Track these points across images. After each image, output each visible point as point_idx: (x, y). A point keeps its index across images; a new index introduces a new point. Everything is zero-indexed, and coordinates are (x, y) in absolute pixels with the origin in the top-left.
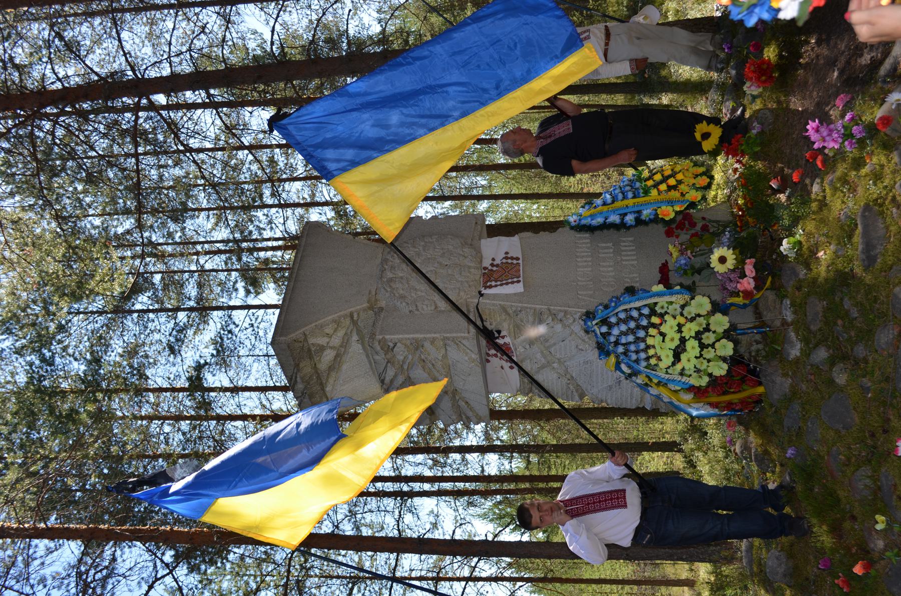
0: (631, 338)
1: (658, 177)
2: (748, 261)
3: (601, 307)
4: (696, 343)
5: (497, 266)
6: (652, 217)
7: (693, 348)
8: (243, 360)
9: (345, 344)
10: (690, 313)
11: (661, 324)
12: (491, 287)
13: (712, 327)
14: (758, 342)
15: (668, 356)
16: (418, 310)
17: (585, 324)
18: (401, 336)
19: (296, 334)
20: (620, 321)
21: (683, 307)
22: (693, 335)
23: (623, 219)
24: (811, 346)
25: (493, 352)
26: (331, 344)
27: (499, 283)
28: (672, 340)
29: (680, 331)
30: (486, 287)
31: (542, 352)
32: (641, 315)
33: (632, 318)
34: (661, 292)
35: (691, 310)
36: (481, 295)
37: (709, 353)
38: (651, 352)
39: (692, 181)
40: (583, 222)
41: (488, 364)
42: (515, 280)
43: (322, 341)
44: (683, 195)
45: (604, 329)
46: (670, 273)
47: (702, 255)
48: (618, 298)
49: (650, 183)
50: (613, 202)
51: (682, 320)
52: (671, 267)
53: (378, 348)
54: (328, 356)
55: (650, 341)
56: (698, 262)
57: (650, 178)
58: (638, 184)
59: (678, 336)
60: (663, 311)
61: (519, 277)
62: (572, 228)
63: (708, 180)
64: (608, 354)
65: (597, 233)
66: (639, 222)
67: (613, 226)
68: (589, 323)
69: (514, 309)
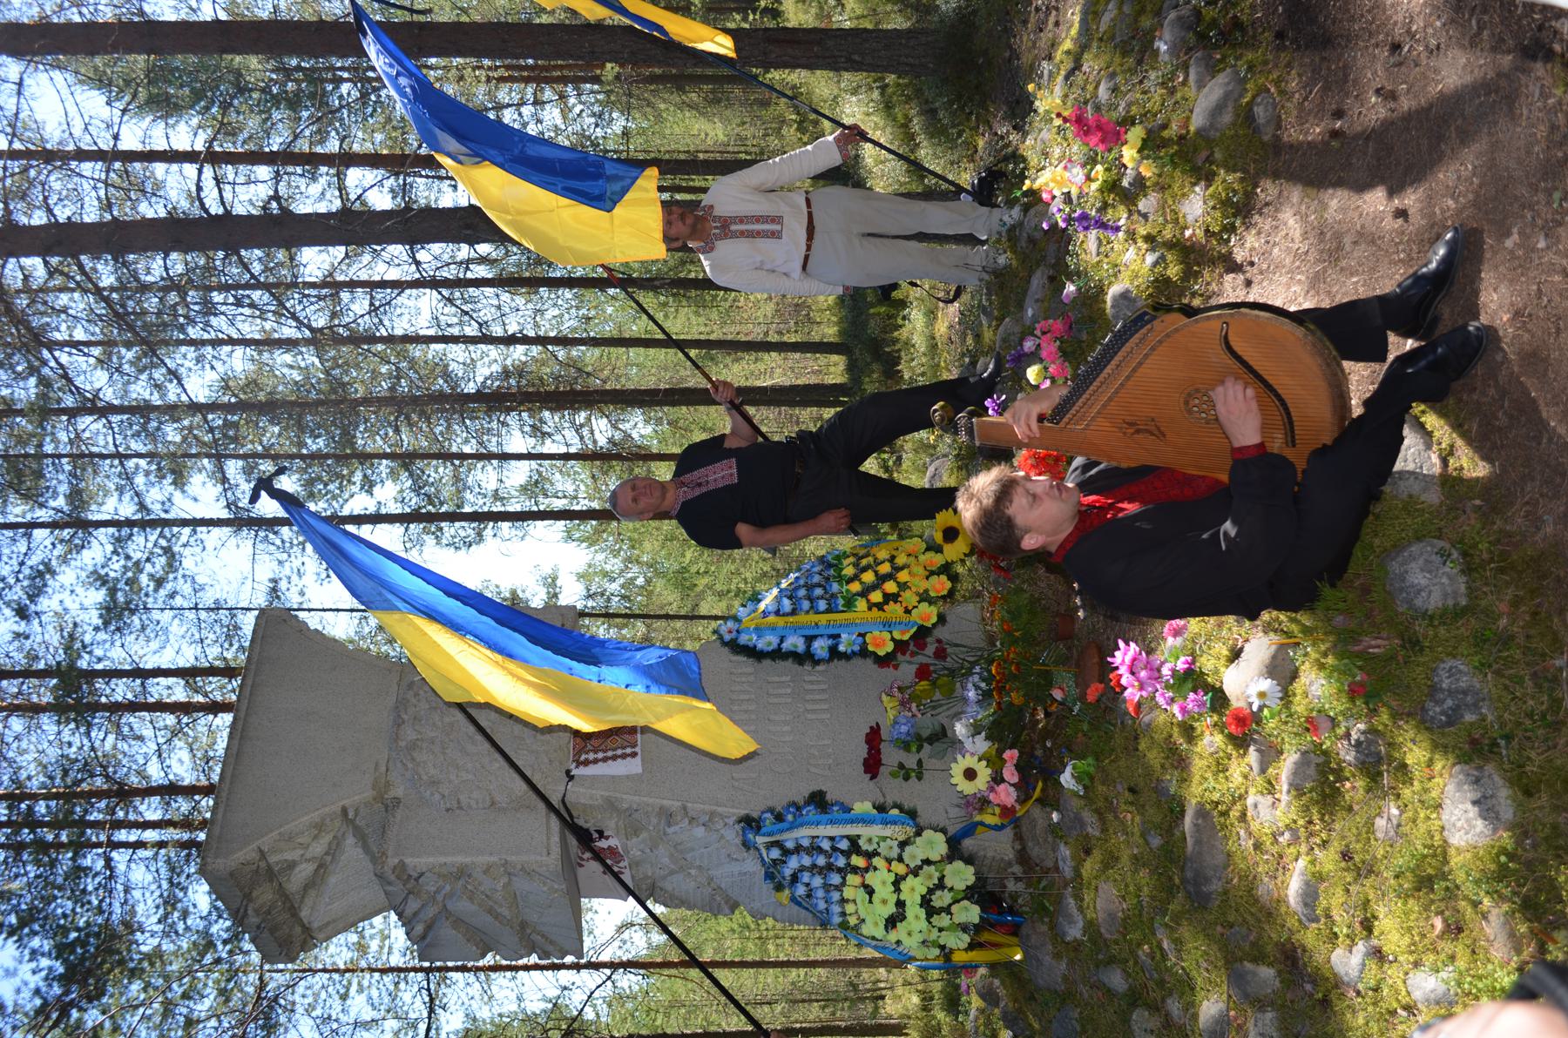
0: (817, 881)
1: (869, 577)
2: (1007, 754)
3: (768, 815)
4: (922, 913)
6: (856, 648)
7: (917, 917)
8: (156, 615)
9: (334, 850)
10: (913, 857)
11: (867, 870)
12: (586, 763)
13: (948, 882)
14: (1018, 879)
15: (876, 924)
16: (460, 808)
17: (744, 834)
18: (431, 860)
19: (244, 854)
20: (798, 849)
21: (903, 845)
22: (919, 900)
23: (809, 647)
24: (1100, 957)
25: (588, 855)
26: (308, 856)
27: (600, 755)
28: (884, 902)
29: (898, 890)
30: (579, 764)
31: (671, 856)
32: (834, 849)
33: (820, 850)
34: (868, 814)
35: (915, 854)
36: (571, 778)
37: (944, 920)
38: (850, 908)
39: (923, 585)
40: (743, 639)
41: (580, 871)
42: (629, 751)
43: (289, 856)
44: (908, 611)
45: (775, 853)
46: (882, 746)
47: (934, 708)
48: (799, 808)
49: (855, 587)
50: (793, 612)
51: (900, 869)
52: (884, 734)
53: (393, 878)
54: (304, 871)
55: (848, 893)
56: (927, 724)
58: (835, 587)
59: (893, 898)
60: (870, 849)
61: (634, 746)
62: (725, 644)
63: (949, 585)
64: (779, 888)
65: (767, 663)
66: (834, 653)
67: (794, 656)
68: (751, 836)
69: (625, 806)
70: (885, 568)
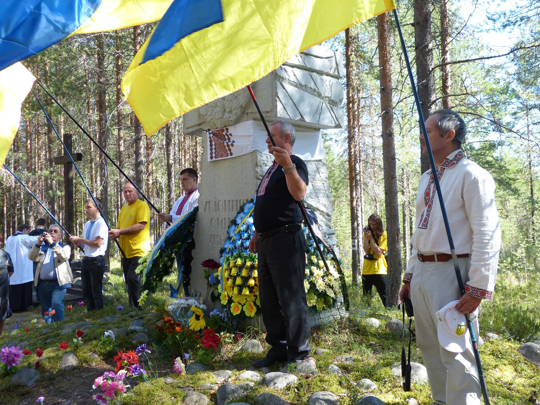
5: (229, 139)
12: (210, 137)
42: (214, 155)
61: (216, 157)
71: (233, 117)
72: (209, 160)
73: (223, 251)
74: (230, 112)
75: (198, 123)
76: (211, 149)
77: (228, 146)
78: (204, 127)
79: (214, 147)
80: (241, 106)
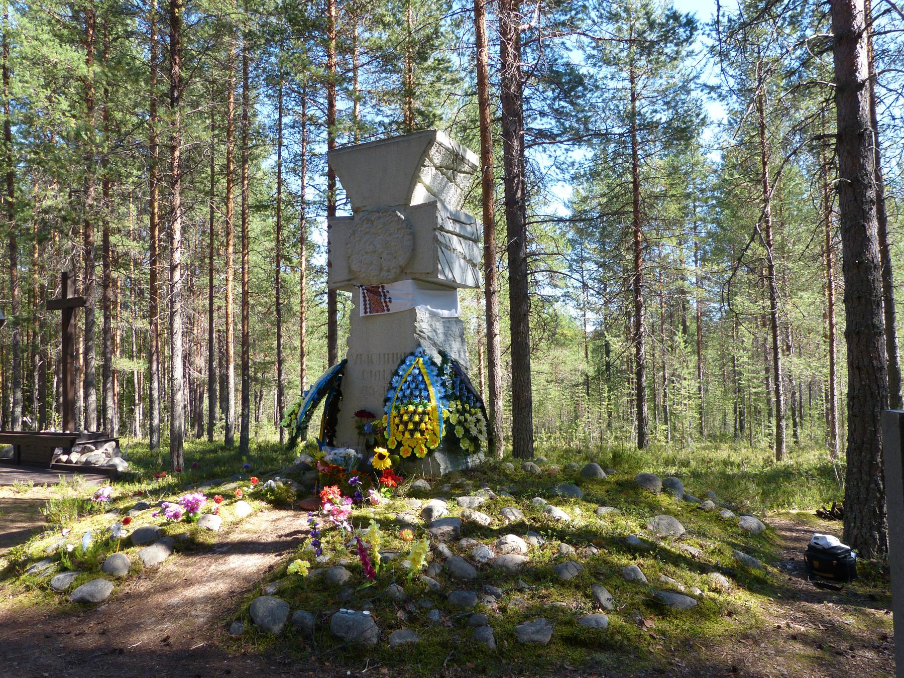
1: (406, 418)
5: (385, 296)
42: (368, 310)
57: (407, 412)
70: (411, 426)
71: (391, 276)
72: (362, 314)
73: (387, 400)
74: (388, 271)
75: (348, 278)
76: (365, 305)
77: (386, 302)
78: (354, 283)
79: (368, 302)
80: (401, 267)
